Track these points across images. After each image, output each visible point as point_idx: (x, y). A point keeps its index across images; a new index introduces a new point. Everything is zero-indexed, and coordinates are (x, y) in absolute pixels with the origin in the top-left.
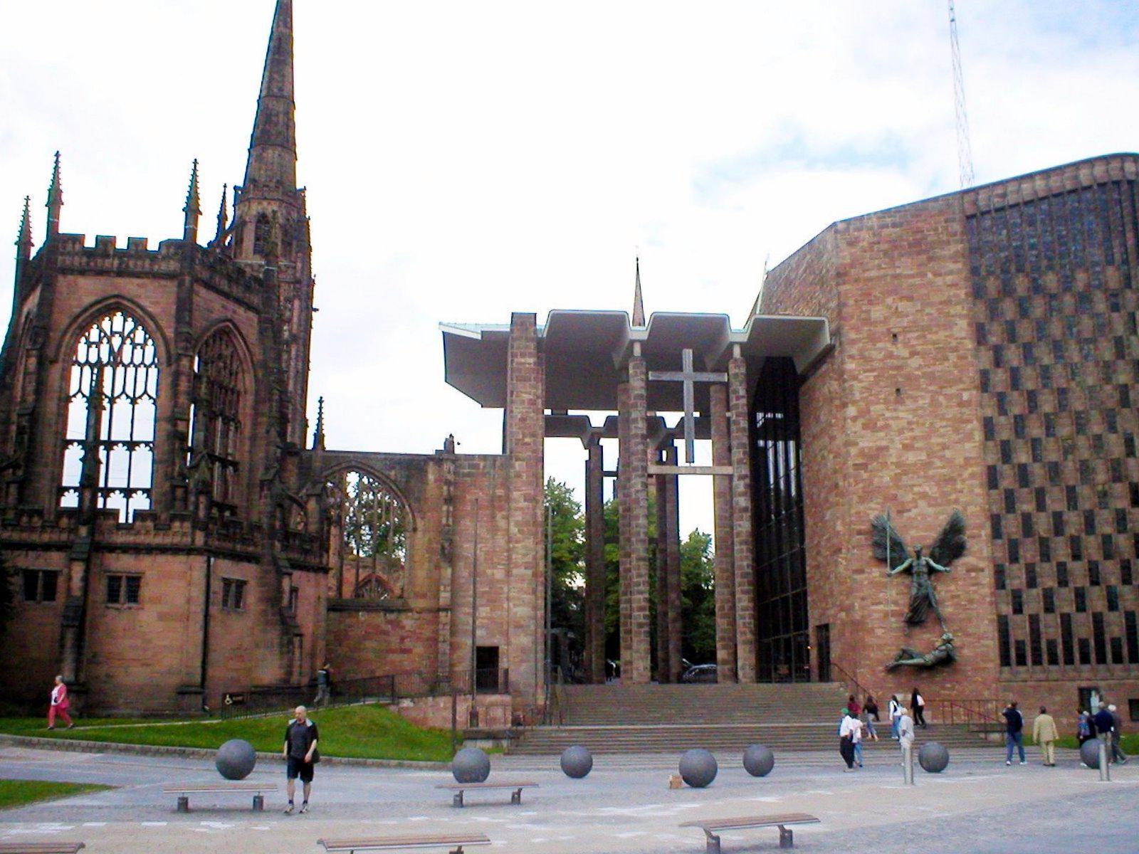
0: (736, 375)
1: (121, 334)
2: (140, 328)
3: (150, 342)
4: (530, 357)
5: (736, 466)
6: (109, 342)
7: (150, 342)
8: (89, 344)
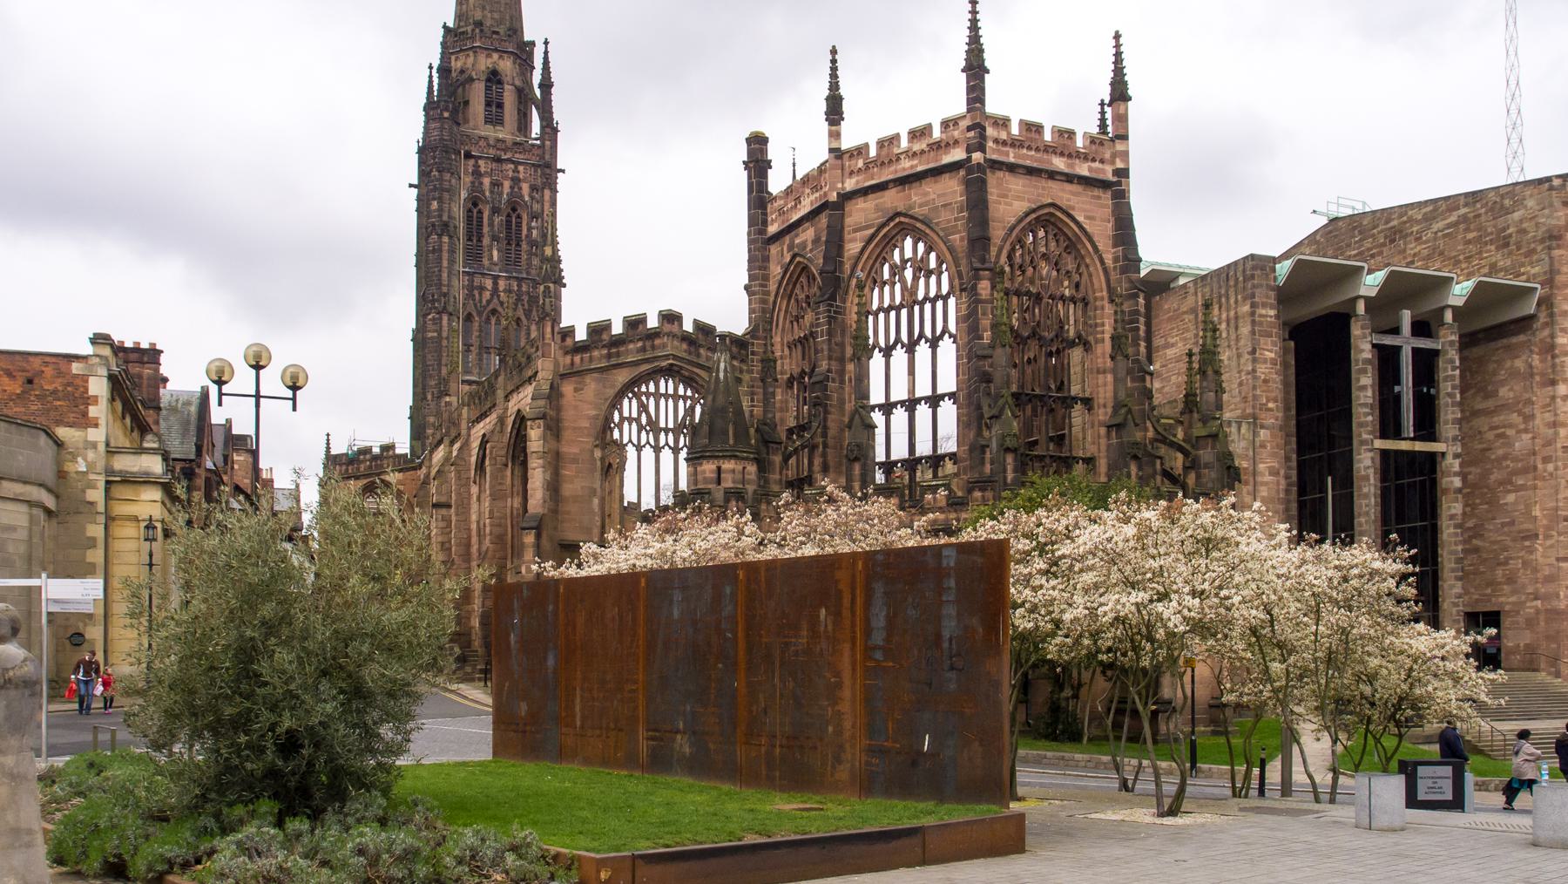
0: (1452, 343)
4: (1271, 308)
5: (1450, 443)
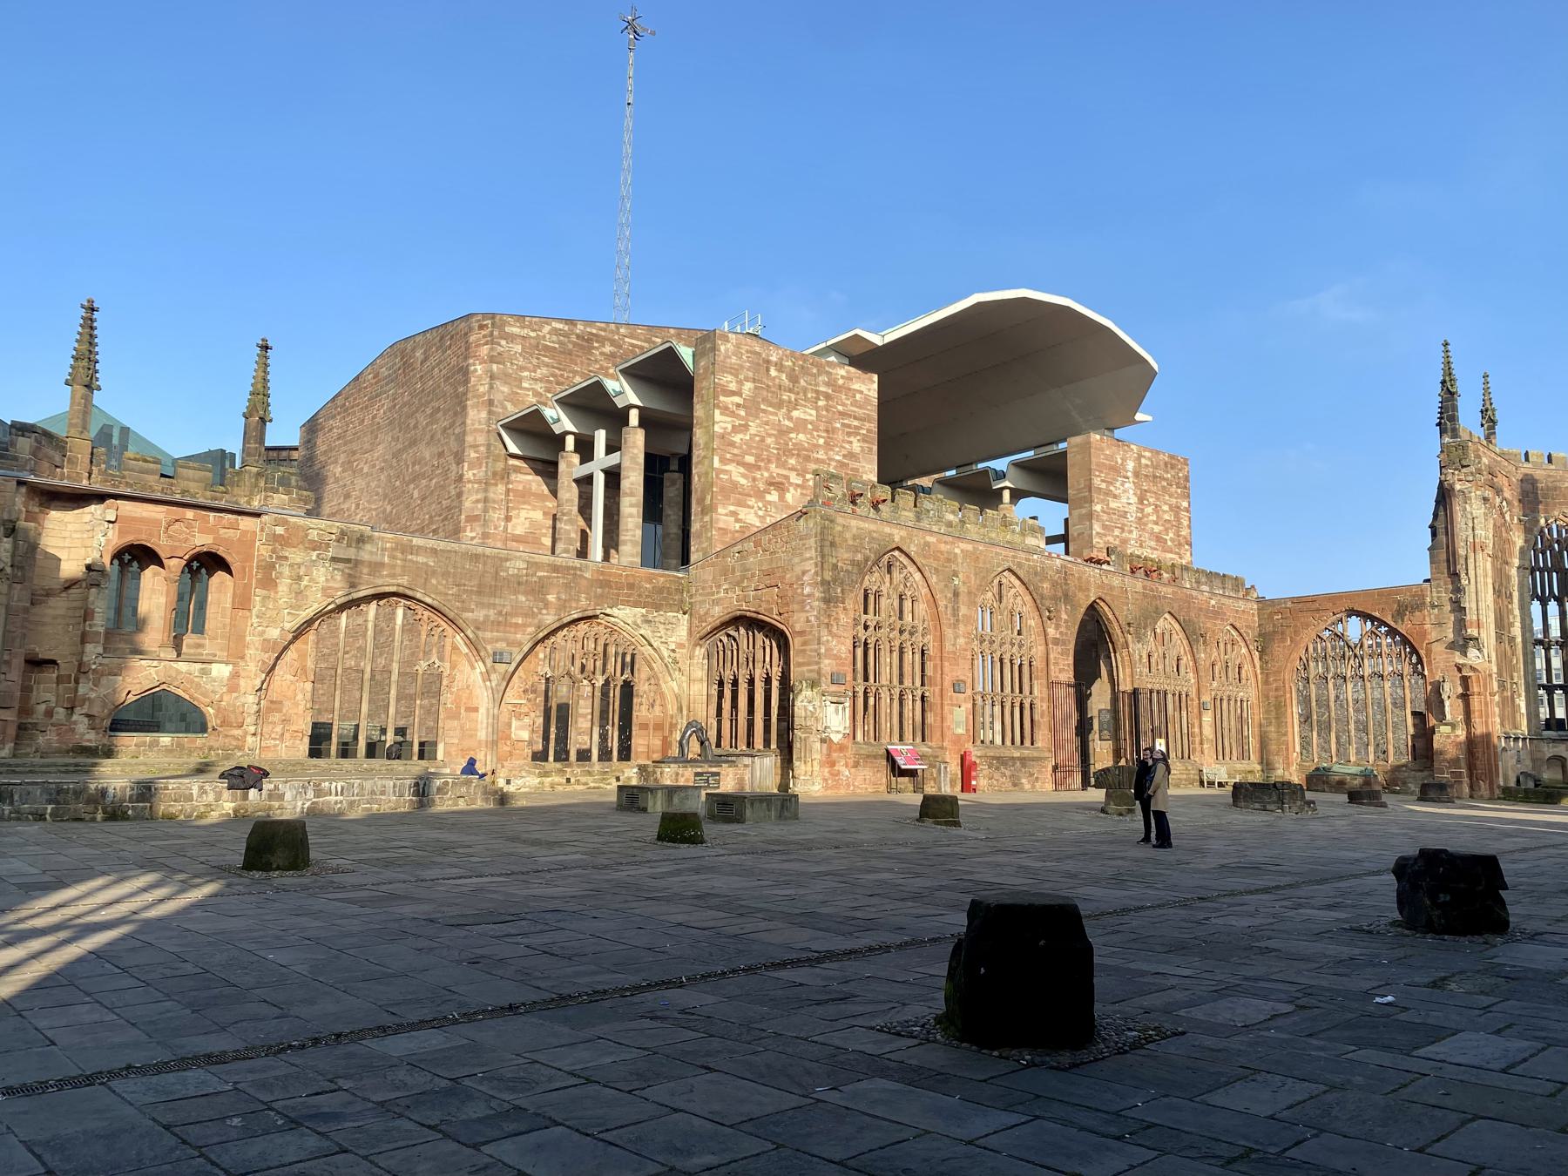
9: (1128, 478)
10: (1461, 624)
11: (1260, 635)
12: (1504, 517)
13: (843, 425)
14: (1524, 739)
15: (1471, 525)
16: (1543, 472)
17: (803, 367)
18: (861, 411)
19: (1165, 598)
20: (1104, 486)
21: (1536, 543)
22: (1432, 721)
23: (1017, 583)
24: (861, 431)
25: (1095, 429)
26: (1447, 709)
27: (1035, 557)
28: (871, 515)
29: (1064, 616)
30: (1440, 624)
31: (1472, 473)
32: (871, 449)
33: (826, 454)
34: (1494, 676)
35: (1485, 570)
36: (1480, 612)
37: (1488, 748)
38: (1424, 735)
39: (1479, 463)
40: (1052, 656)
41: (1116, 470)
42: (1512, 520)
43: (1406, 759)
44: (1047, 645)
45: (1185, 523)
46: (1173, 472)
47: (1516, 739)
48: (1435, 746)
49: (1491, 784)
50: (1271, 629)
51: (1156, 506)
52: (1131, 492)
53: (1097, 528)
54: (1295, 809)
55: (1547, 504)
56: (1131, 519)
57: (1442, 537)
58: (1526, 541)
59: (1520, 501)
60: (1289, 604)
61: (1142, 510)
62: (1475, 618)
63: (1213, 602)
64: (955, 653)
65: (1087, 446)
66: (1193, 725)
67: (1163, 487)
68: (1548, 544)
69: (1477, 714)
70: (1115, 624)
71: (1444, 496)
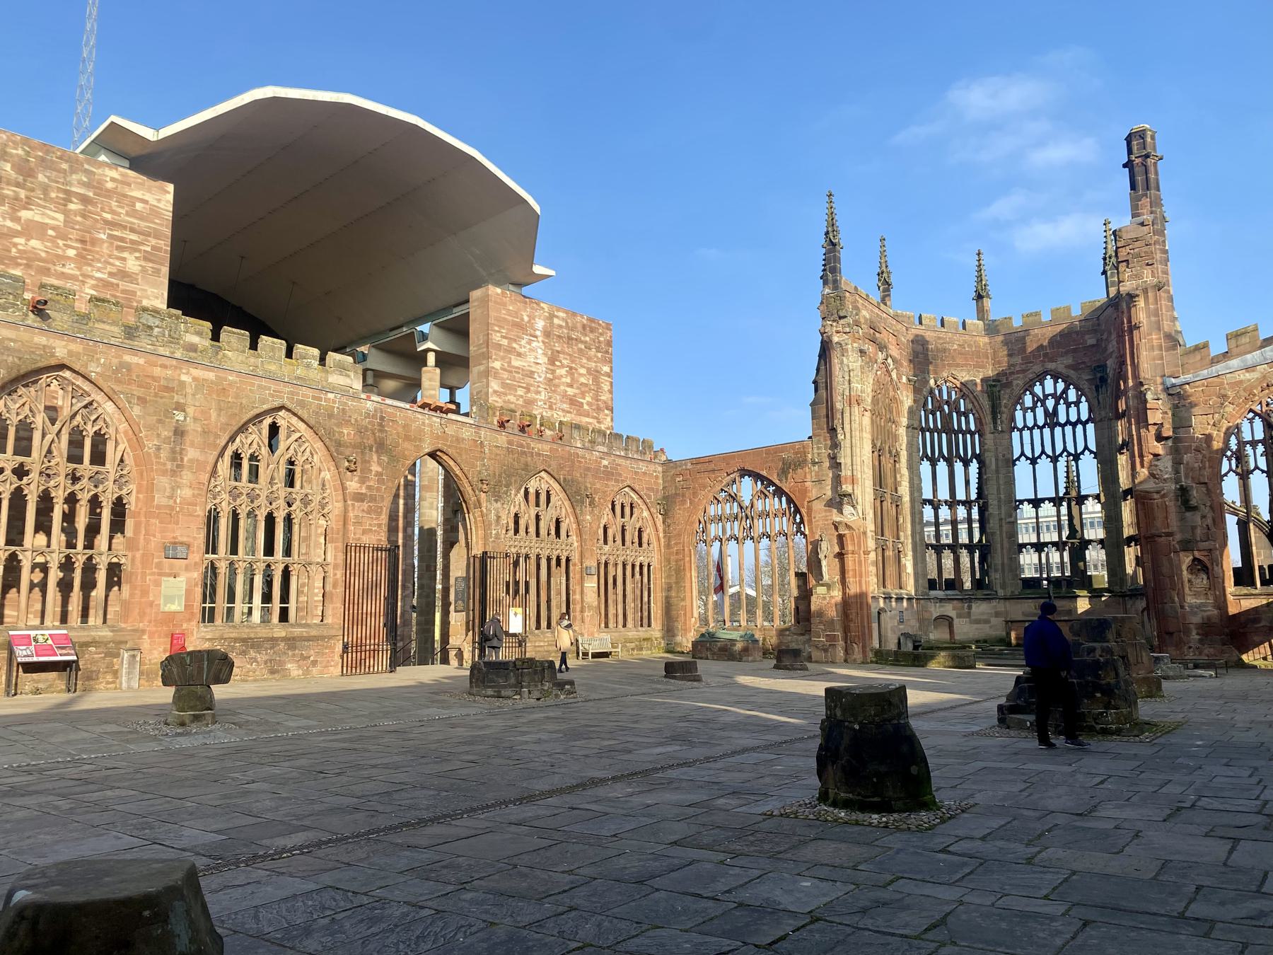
1: (1054, 395)
2: (1072, 387)
3: (1083, 399)
6: (1043, 405)
7: (1083, 399)
8: (1025, 410)
9: (536, 337)
10: (837, 480)
11: (665, 498)
12: (890, 376)
13: (110, 236)
14: (909, 599)
15: (847, 378)
16: (933, 334)
17: (43, 160)
18: (143, 224)
19: (539, 455)
20: (505, 342)
21: (925, 404)
22: (812, 582)
23: (302, 426)
24: (142, 248)
25: (498, 283)
26: (824, 569)
27: (331, 396)
28: (29, 322)
29: (375, 468)
30: (820, 481)
31: (849, 324)
32: (157, 272)
33: (79, 269)
34: (870, 534)
35: (861, 424)
36: (855, 467)
37: (861, 609)
38: (805, 595)
39: (857, 314)
40: (351, 514)
41: (522, 328)
42: (899, 378)
43: (791, 620)
44: (345, 501)
45: (606, 387)
46: (592, 336)
47: (900, 599)
48: (813, 608)
49: (864, 647)
50: (674, 492)
51: (571, 368)
52: (540, 351)
53: (494, 385)
54: (536, 694)
55: (936, 366)
56: (538, 379)
57: (823, 392)
58: (915, 401)
59: (910, 361)
60: (689, 466)
61: (553, 372)
62: (849, 473)
63: (605, 462)
64: (172, 508)
65: (485, 300)
66: (574, 592)
67: (580, 350)
68: (937, 405)
69: (851, 573)
70: (465, 481)
71: (826, 350)
